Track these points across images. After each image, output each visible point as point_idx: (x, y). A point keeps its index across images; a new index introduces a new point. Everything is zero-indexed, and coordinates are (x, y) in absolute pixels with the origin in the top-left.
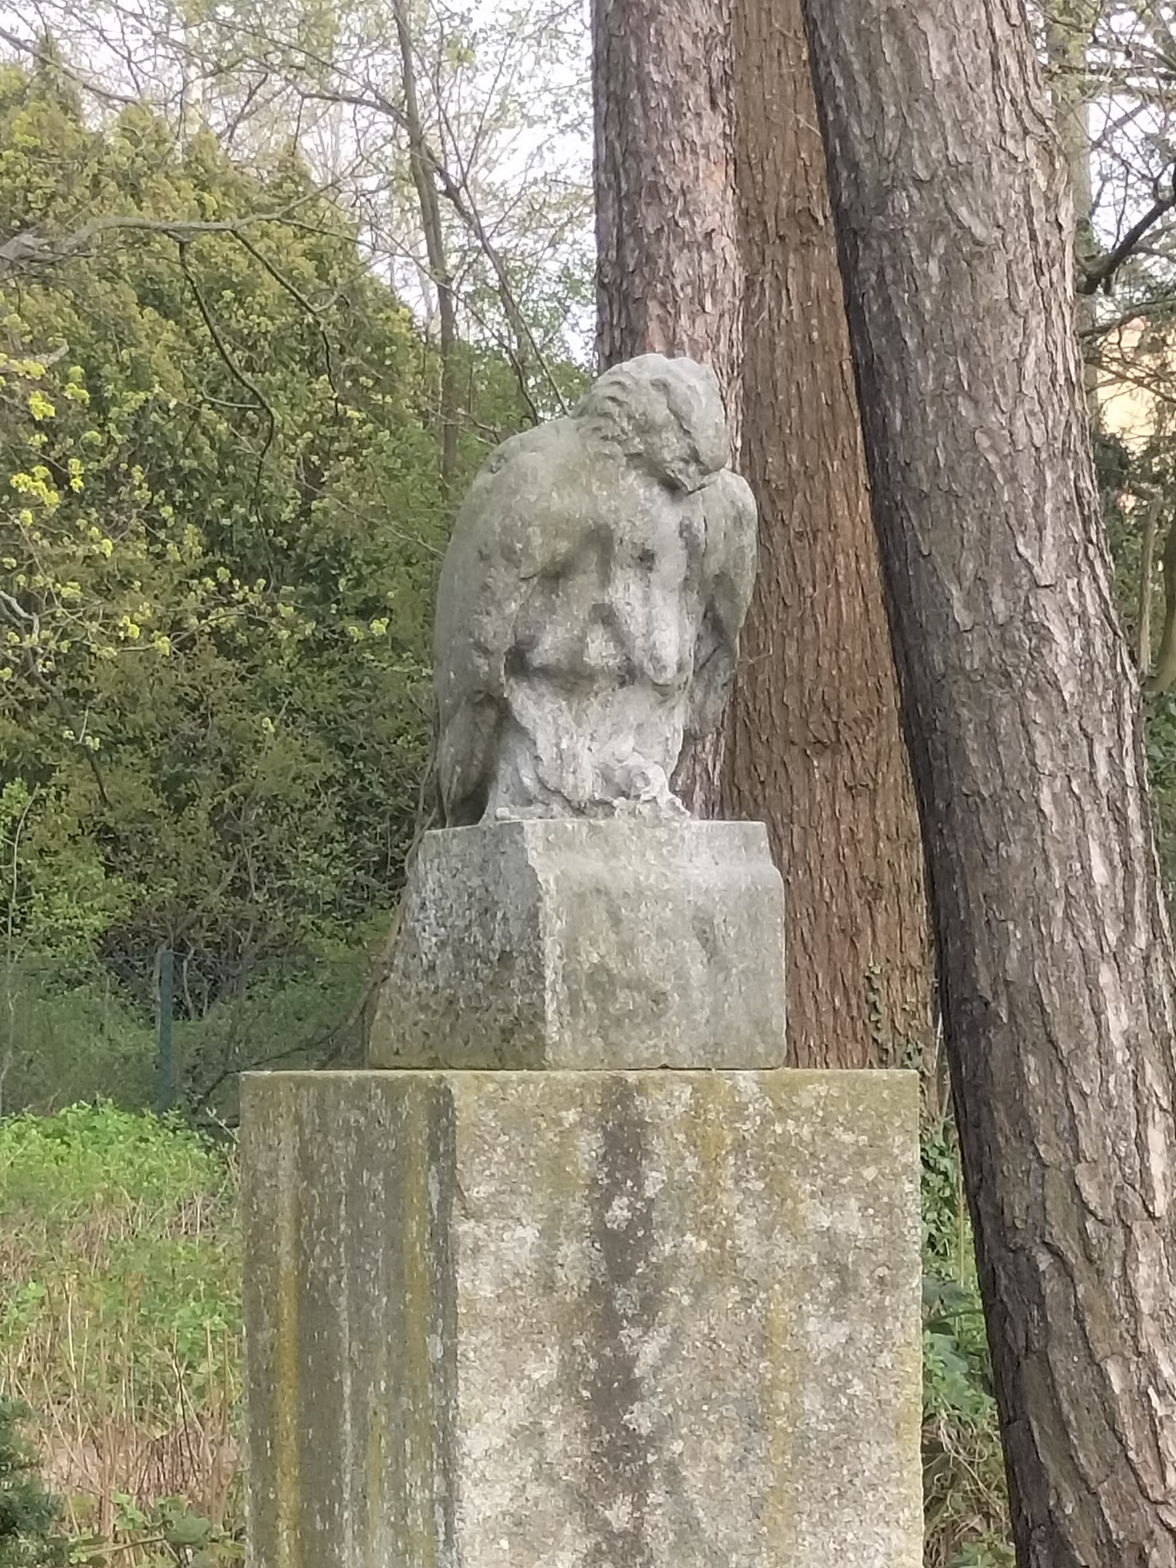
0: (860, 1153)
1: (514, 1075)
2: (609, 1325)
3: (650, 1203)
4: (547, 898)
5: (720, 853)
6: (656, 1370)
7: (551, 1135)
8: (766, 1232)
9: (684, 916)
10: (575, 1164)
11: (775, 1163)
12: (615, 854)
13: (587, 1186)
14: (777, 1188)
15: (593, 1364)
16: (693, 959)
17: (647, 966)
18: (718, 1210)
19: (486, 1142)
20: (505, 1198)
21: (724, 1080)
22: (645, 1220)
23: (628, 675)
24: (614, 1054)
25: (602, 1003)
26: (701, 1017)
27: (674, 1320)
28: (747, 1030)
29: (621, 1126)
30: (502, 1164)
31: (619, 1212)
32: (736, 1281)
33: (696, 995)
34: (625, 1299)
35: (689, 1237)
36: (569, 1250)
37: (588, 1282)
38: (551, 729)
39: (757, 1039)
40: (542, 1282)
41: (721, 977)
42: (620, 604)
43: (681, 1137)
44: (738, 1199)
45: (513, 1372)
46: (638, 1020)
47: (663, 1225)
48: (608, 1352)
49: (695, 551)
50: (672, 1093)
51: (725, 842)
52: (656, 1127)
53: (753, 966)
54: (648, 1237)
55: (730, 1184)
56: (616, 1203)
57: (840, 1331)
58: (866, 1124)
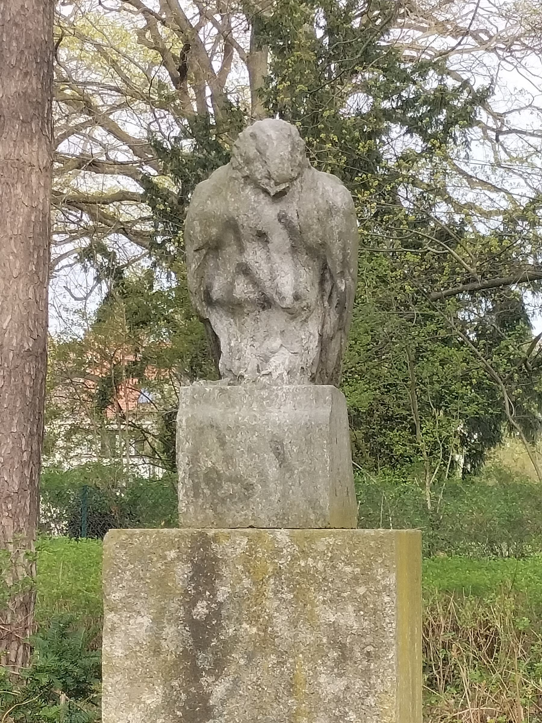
0: (356, 579)
1: (138, 531)
2: (195, 673)
3: (220, 604)
4: (180, 430)
5: (299, 403)
6: (223, 702)
7: (159, 565)
8: (294, 623)
9: (265, 440)
10: (174, 582)
11: (300, 584)
12: (233, 406)
13: (182, 594)
14: (300, 596)
15: (183, 696)
16: (270, 465)
17: (241, 469)
18: (263, 609)
19: (119, 568)
20: (131, 600)
21: (268, 535)
22: (217, 614)
23: (266, 303)
24: (220, 519)
25: (213, 491)
26: (275, 498)
27: (234, 673)
28: (304, 506)
29: (202, 560)
30: (130, 581)
31: (201, 609)
32: (274, 651)
33: (272, 485)
34: (204, 659)
35: (245, 625)
36: (170, 631)
37: (181, 649)
38: (226, 335)
39: (311, 511)
40: (153, 648)
41: (287, 475)
42: (252, 263)
43: (240, 567)
44: (276, 603)
45: (134, 699)
46: (236, 500)
47: (229, 618)
48: (193, 689)
49: (292, 231)
50: (235, 542)
51: (303, 397)
52: (225, 561)
53: (308, 469)
54: (219, 624)
55: (271, 595)
56: (199, 604)
57: (341, 683)
58: (360, 561)
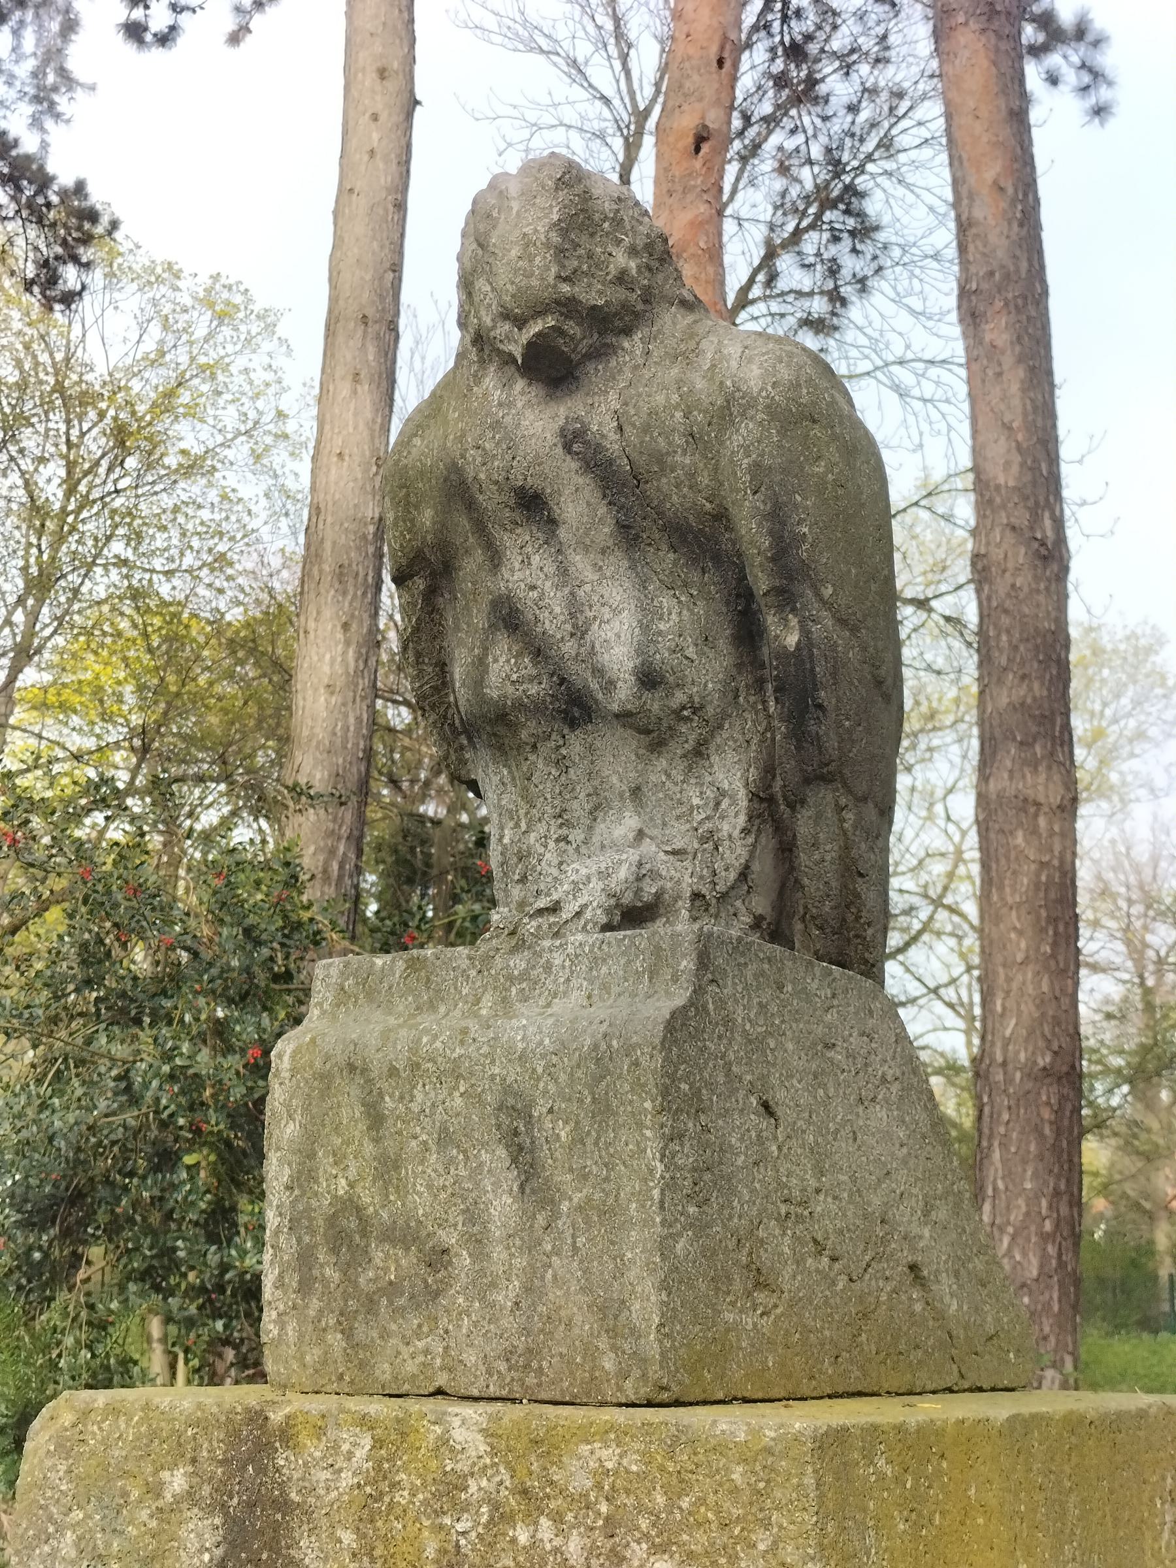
16: (497, 1185)
17: (421, 1202)
25: (348, 1270)
26: (504, 1297)
33: (498, 1253)
39: (603, 1343)
41: (541, 1220)
46: (402, 1301)
